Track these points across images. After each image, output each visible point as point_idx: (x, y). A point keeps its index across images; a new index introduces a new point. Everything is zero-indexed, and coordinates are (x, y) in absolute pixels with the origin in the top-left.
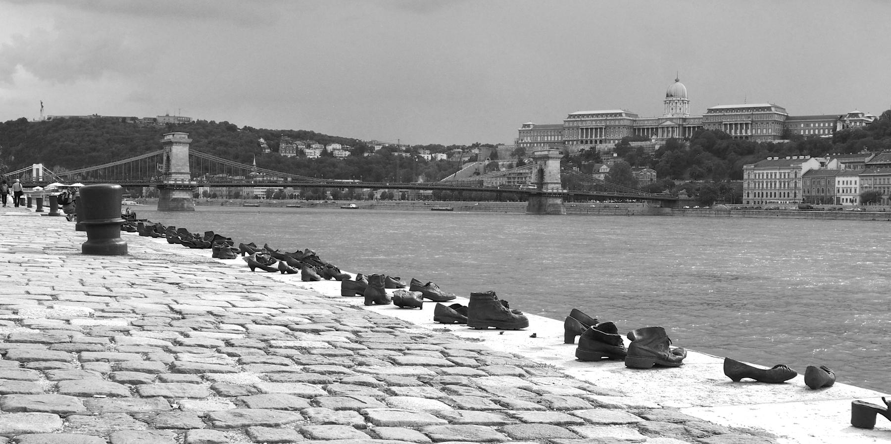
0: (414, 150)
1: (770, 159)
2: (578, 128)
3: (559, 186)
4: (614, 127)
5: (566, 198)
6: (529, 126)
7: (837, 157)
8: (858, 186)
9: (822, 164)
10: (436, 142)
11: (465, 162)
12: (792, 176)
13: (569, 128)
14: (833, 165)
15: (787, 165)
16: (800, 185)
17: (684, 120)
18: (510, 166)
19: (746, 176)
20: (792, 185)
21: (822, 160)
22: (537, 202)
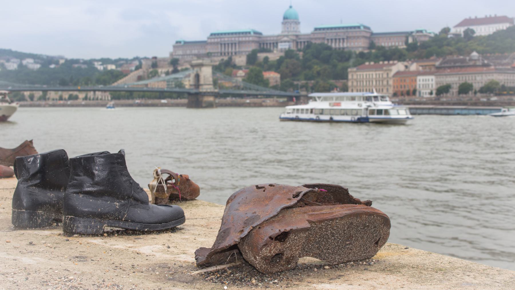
0: (90, 63)
1: (367, 63)
2: (217, 43)
3: (211, 86)
4: (245, 42)
5: (216, 95)
6: (180, 42)
7: (416, 62)
8: (434, 82)
9: (406, 67)
10: (105, 56)
11: (132, 71)
12: (385, 76)
13: (211, 44)
14: (414, 67)
15: (381, 68)
16: (391, 82)
17: (297, 36)
18: (167, 73)
19: (350, 77)
20: (385, 83)
21: (406, 63)
22: (195, 100)
